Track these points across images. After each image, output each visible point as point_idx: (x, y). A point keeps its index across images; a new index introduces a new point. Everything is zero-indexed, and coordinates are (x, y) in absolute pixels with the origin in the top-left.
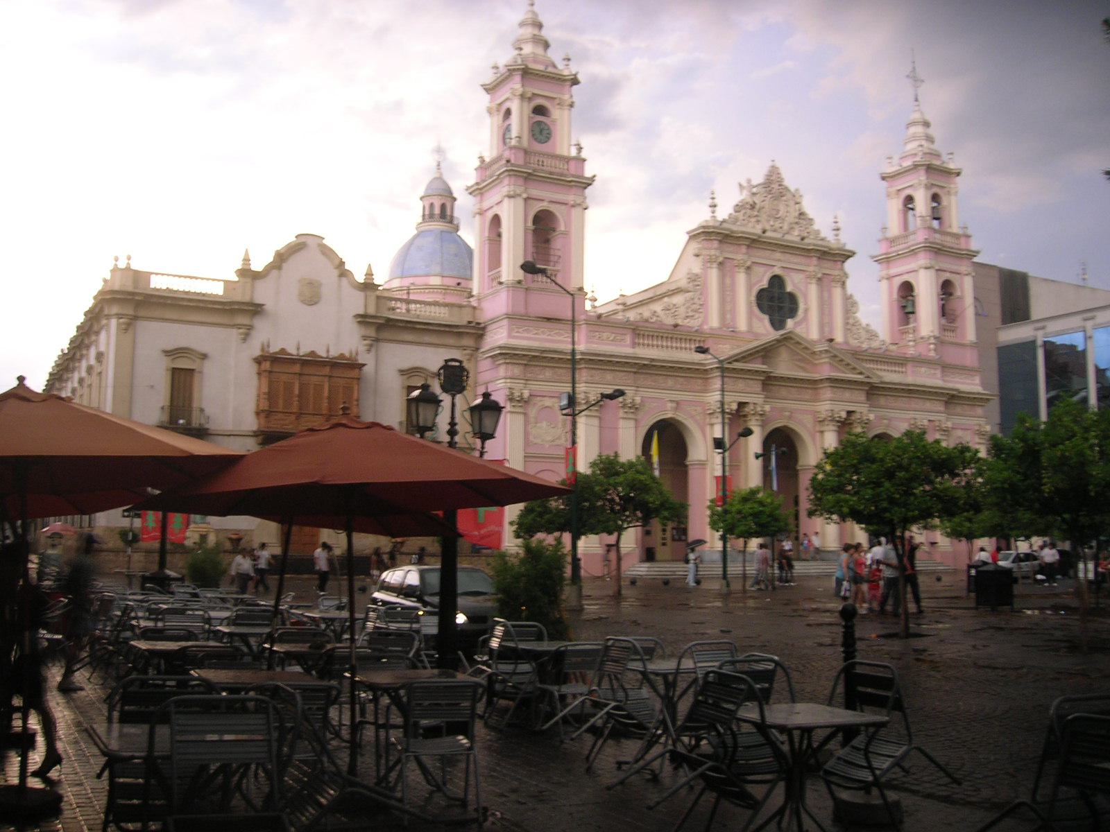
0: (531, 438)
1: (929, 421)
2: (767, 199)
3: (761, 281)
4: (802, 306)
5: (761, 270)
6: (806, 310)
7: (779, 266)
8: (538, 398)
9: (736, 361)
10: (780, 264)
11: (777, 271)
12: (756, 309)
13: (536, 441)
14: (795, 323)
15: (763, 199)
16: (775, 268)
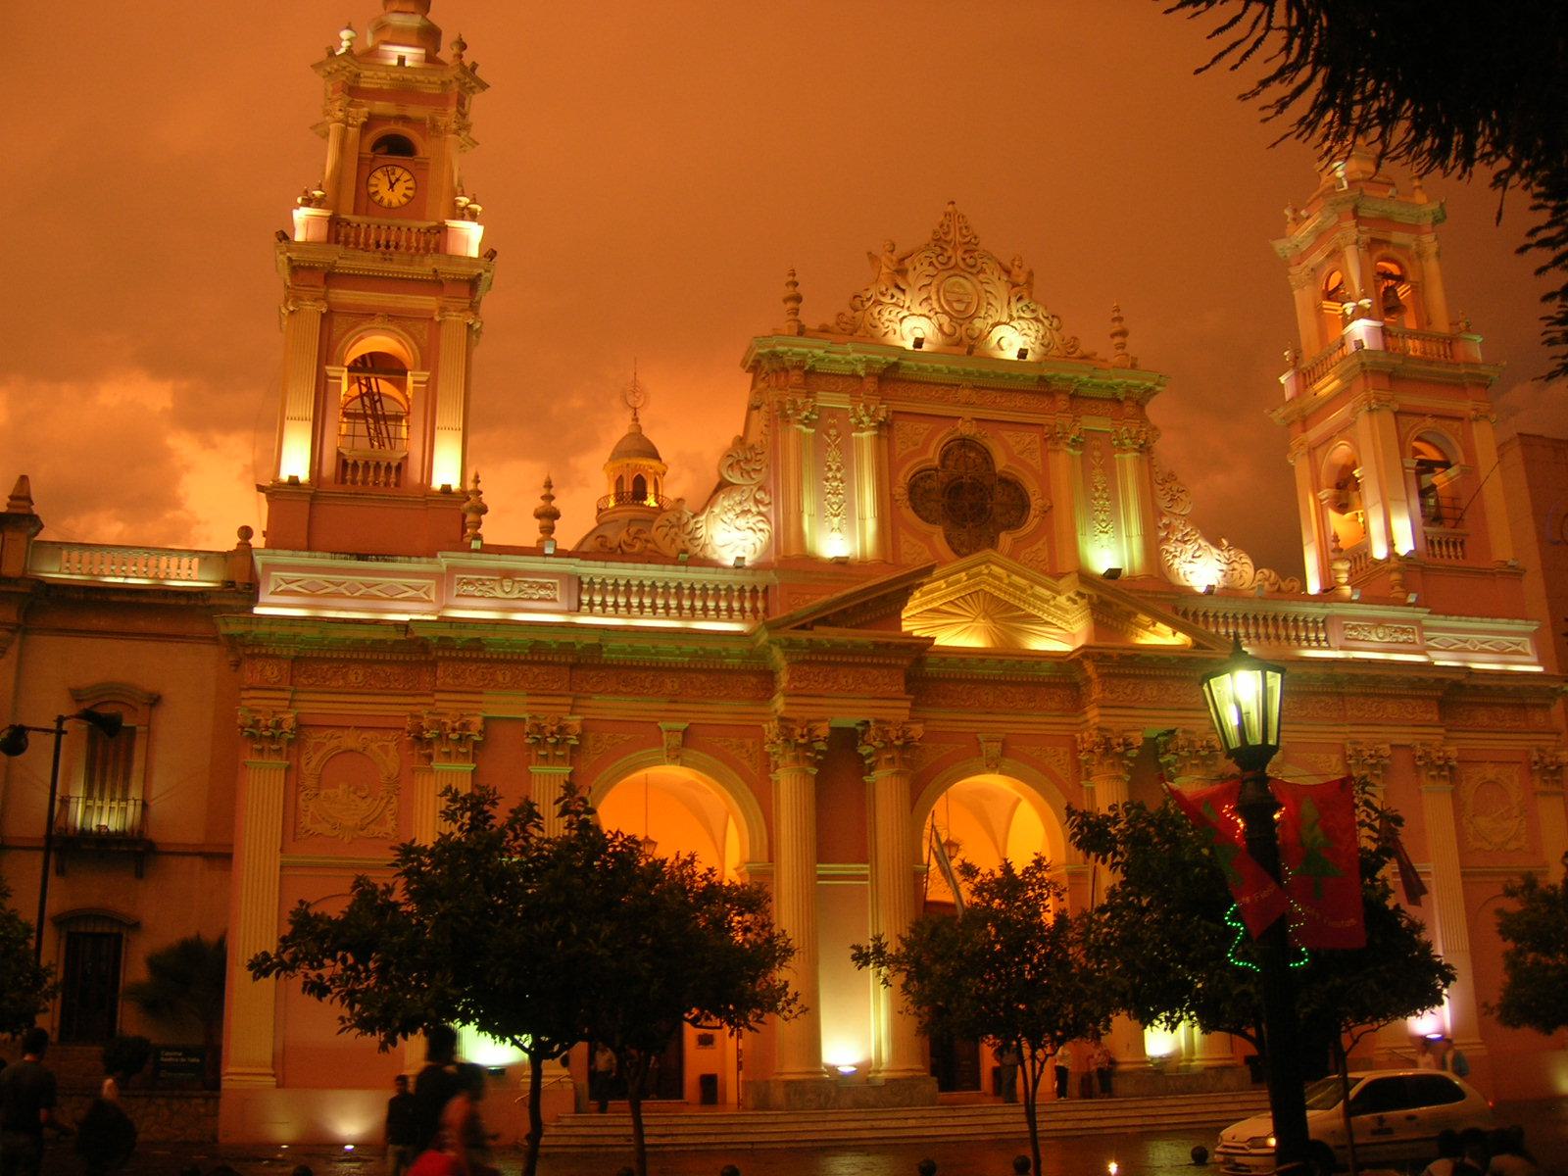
0: (306, 821)
1: (1392, 746)
2: (935, 282)
3: (924, 450)
4: (1036, 503)
5: (924, 427)
6: (1047, 511)
7: (968, 417)
8: (330, 731)
9: (824, 621)
10: (968, 413)
11: (966, 429)
12: (909, 514)
13: (319, 828)
14: (1016, 541)
15: (927, 281)
16: (960, 421)
